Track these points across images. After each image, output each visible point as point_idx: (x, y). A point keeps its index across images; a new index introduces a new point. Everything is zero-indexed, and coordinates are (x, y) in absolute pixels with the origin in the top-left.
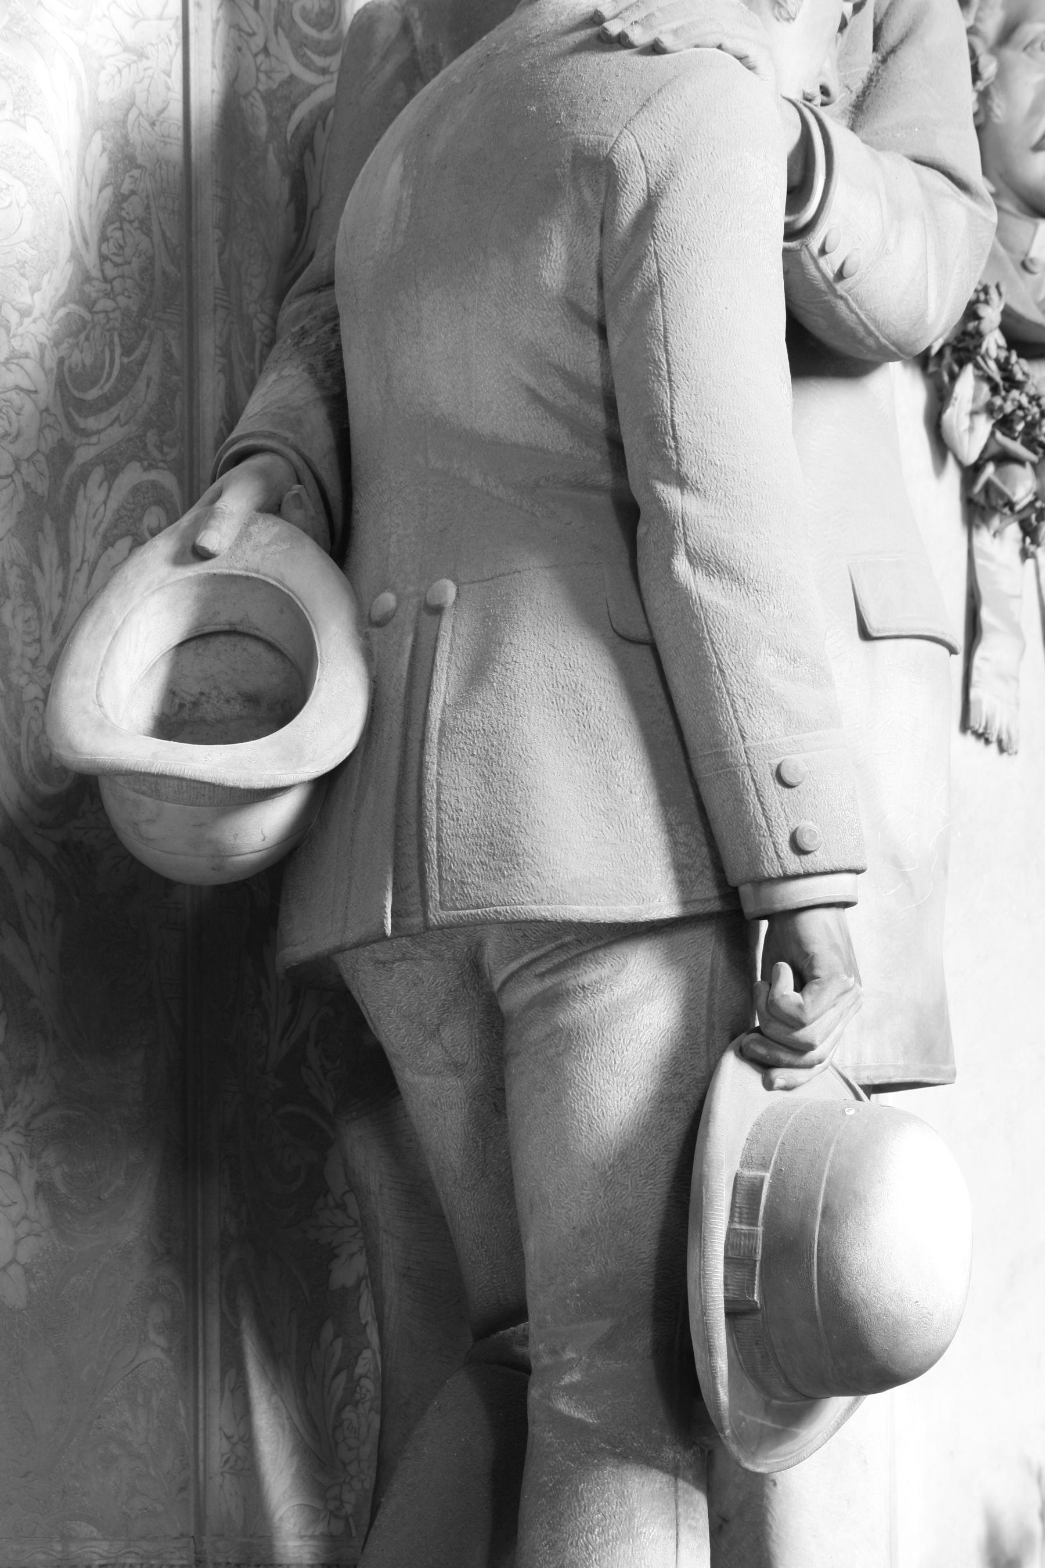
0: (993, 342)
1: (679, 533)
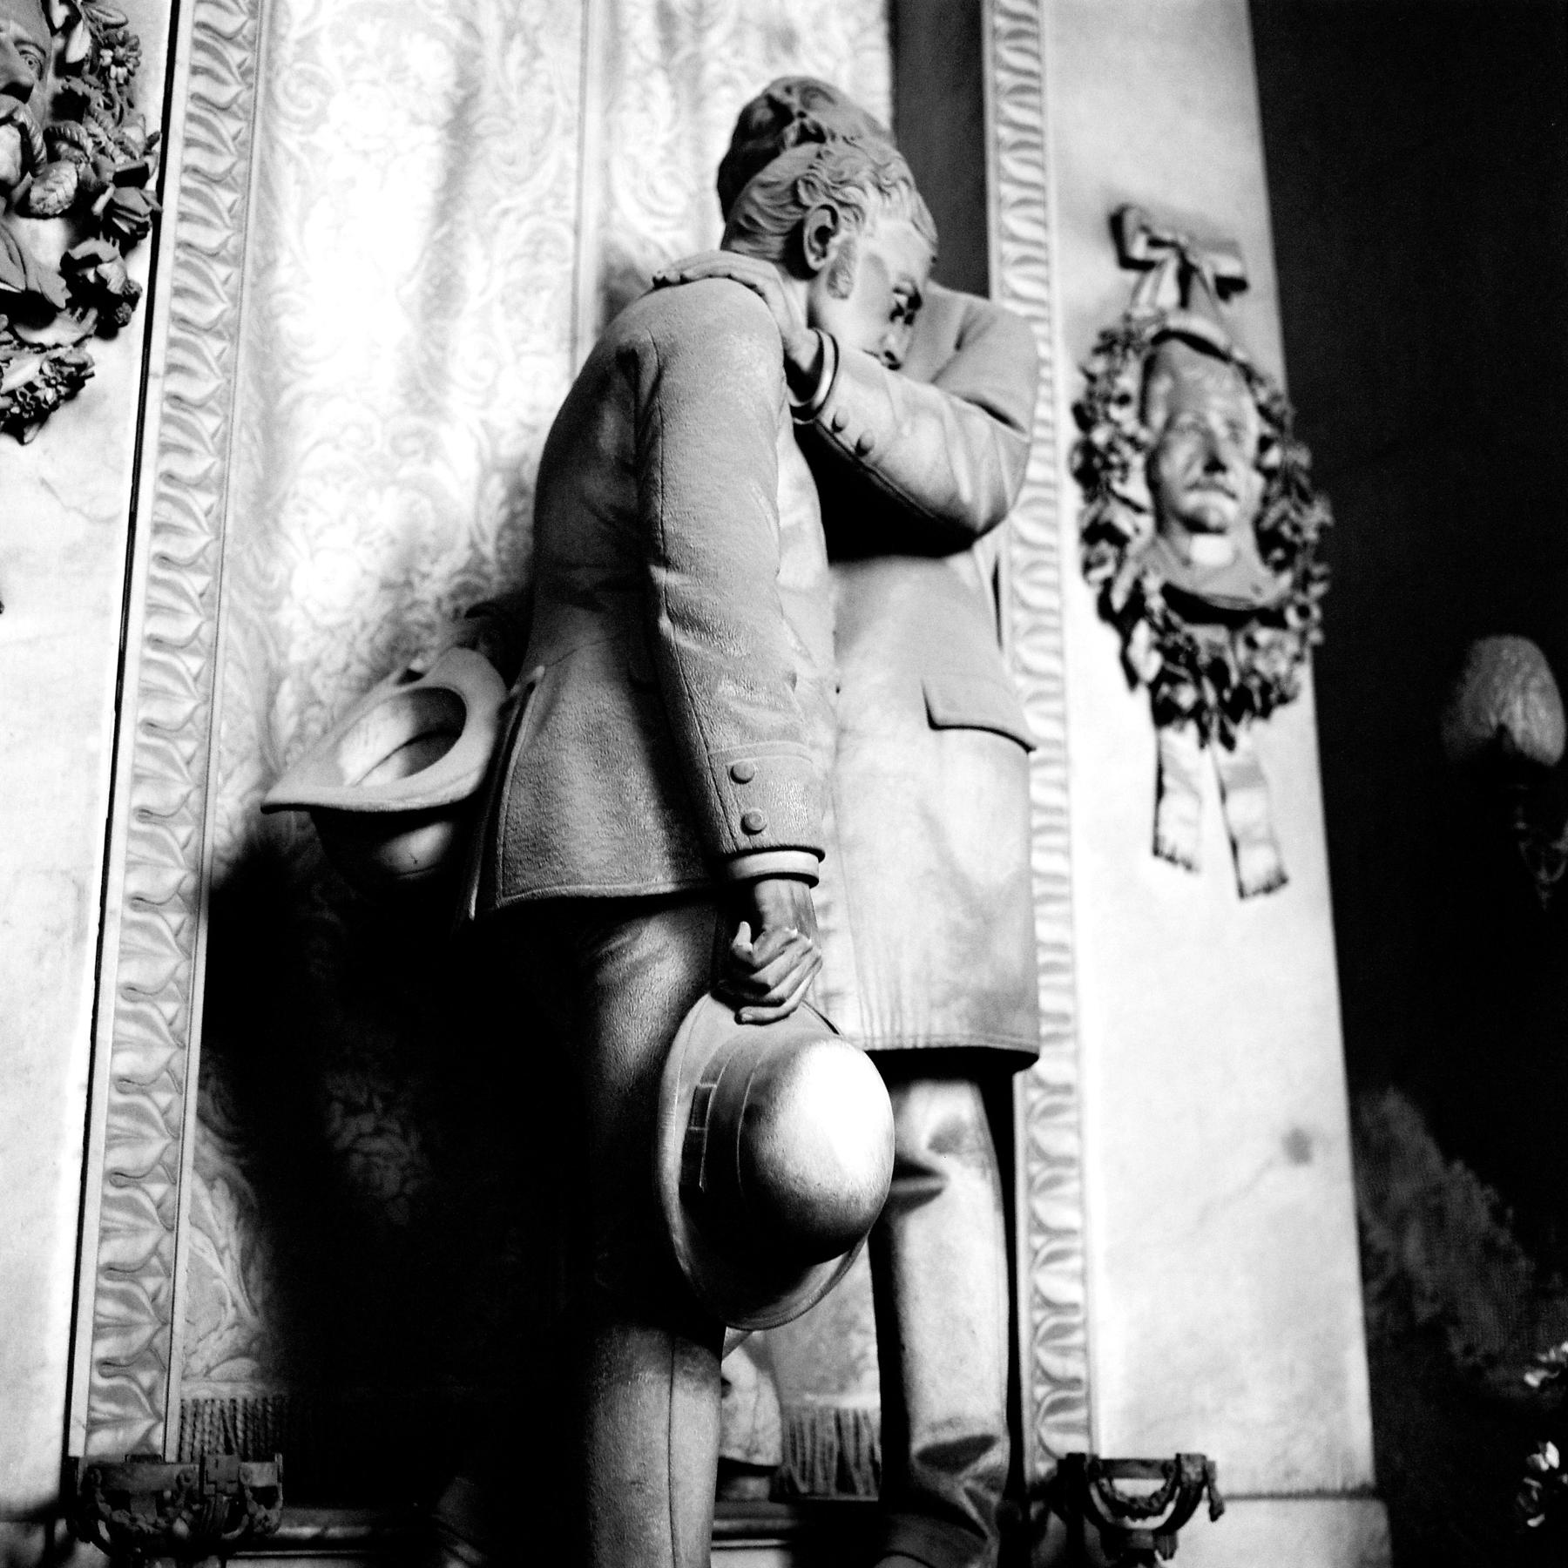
0: (1156, 603)
1: (663, 599)
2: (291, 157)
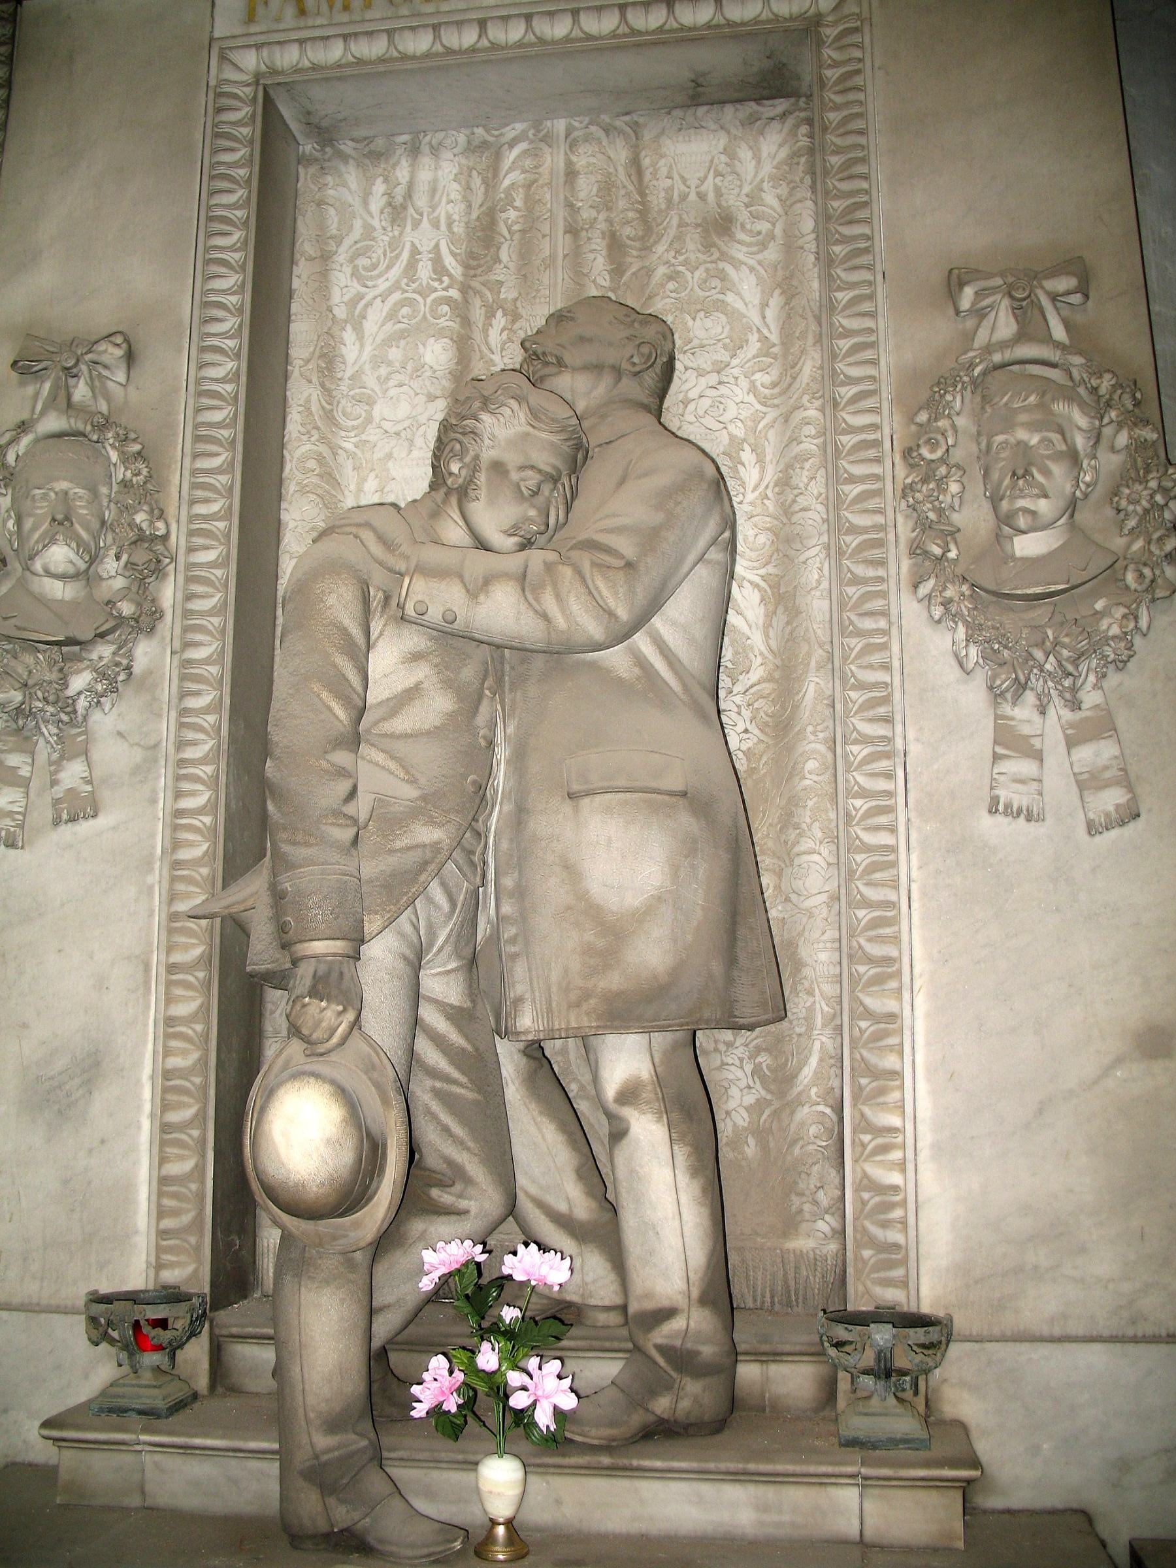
2: (351, 455)
